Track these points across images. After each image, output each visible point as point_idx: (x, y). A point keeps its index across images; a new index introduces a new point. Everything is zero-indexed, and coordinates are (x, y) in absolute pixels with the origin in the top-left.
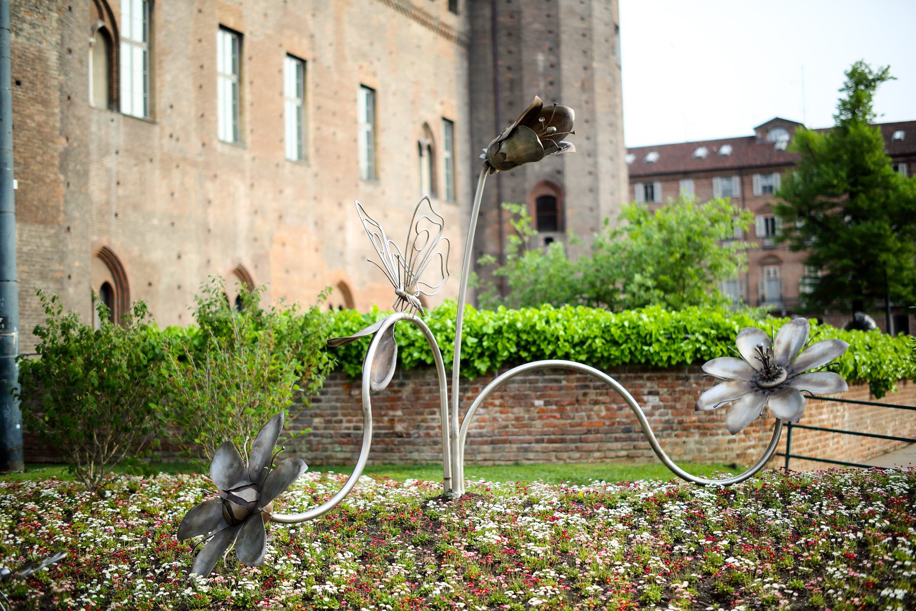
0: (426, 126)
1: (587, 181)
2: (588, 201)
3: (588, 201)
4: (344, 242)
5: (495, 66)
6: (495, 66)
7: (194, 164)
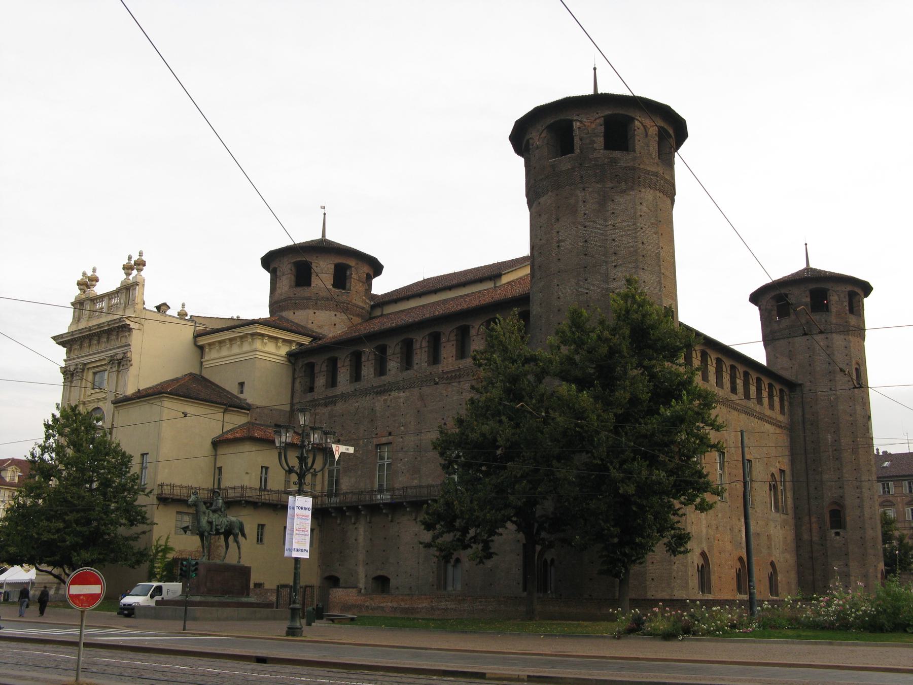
0: (773, 475)
5: (805, 440)
6: (805, 440)
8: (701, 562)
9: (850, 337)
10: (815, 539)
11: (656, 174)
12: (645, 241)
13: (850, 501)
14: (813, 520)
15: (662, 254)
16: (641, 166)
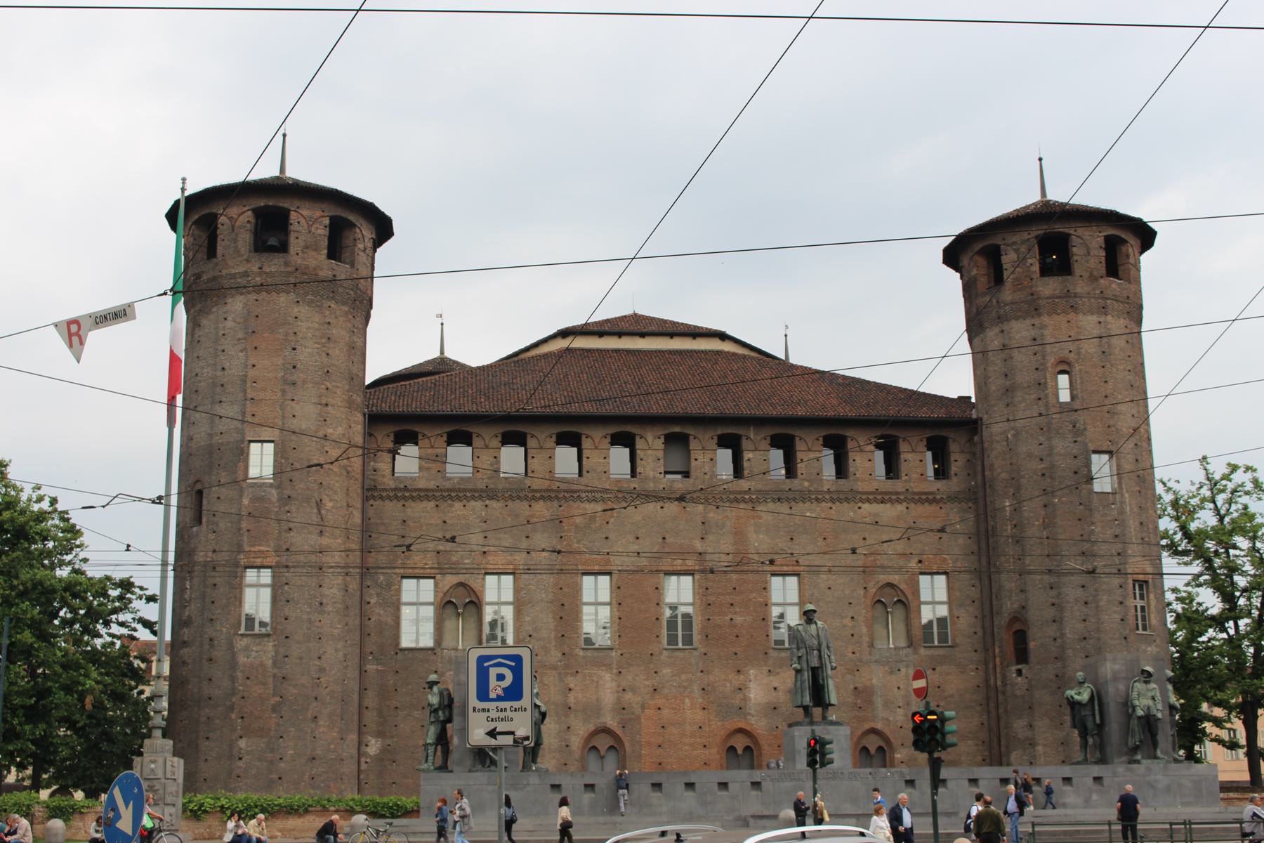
1: (1050, 613)
2: (1052, 630)
3: (1052, 630)
4: (745, 699)
7: (554, 668)
8: (603, 742)
9: (1045, 319)
10: (999, 683)
11: (246, 274)
12: (227, 365)
13: (1039, 611)
14: (997, 651)
15: (251, 372)
16: (224, 272)
